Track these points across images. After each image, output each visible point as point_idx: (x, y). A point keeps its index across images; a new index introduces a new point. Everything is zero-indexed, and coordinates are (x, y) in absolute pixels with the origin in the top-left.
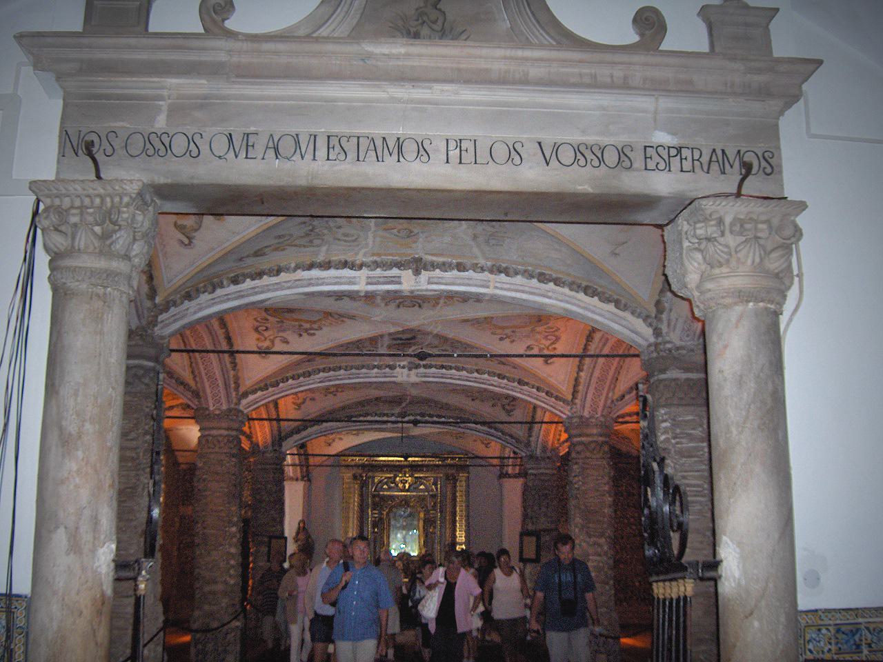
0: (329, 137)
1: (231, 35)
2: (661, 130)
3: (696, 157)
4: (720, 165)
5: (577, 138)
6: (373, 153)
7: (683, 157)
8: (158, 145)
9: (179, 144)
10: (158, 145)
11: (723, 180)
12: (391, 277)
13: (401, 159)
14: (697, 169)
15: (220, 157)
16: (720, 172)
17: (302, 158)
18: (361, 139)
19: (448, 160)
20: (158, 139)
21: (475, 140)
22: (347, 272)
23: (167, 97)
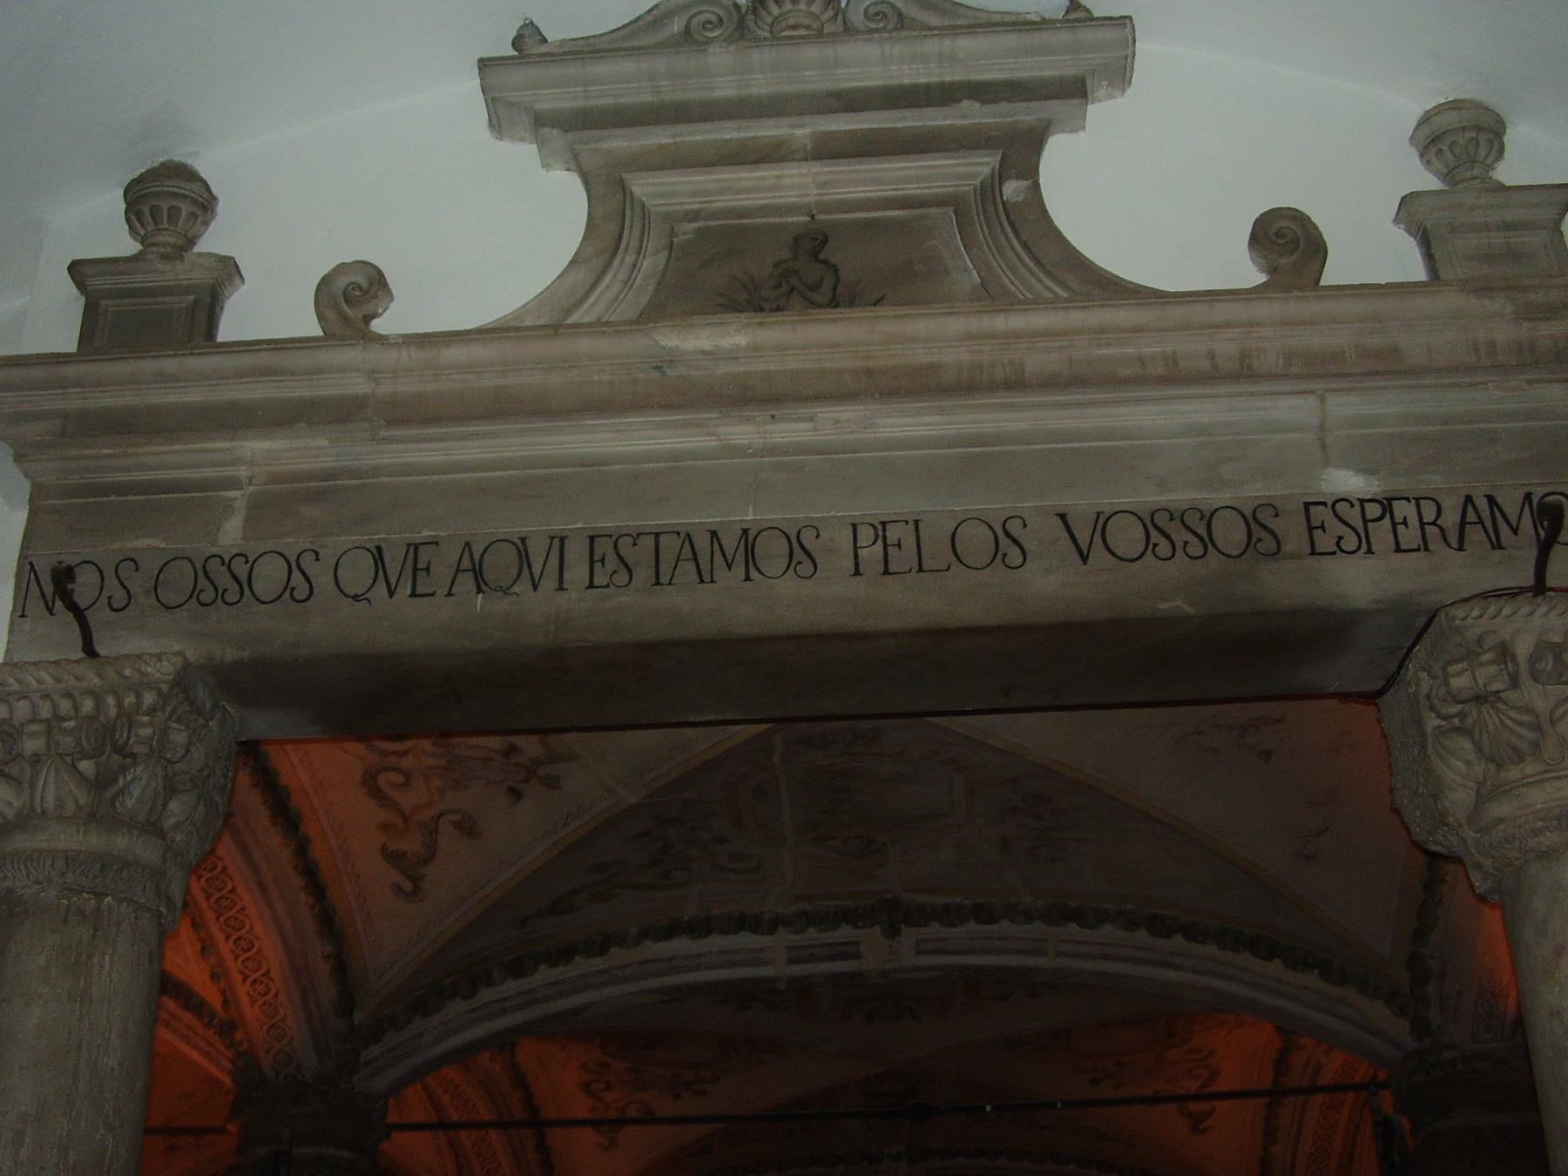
0: (592, 539)
1: (382, 340)
2: (1338, 467)
3: (1429, 515)
4: (1484, 527)
5: (1152, 497)
6: (690, 567)
7: (1399, 519)
8: (223, 579)
9: (270, 575)
10: (223, 579)
11: (1500, 563)
12: (839, 944)
13: (754, 574)
14: (1436, 544)
15: (355, 597)
16: (1489, 547)
17: (535, 587)
18: (662, 539)
19: (857, 565)
20: (225, 567)
21: (917, 522)
22: (746, 940)
23: (245, 481)
